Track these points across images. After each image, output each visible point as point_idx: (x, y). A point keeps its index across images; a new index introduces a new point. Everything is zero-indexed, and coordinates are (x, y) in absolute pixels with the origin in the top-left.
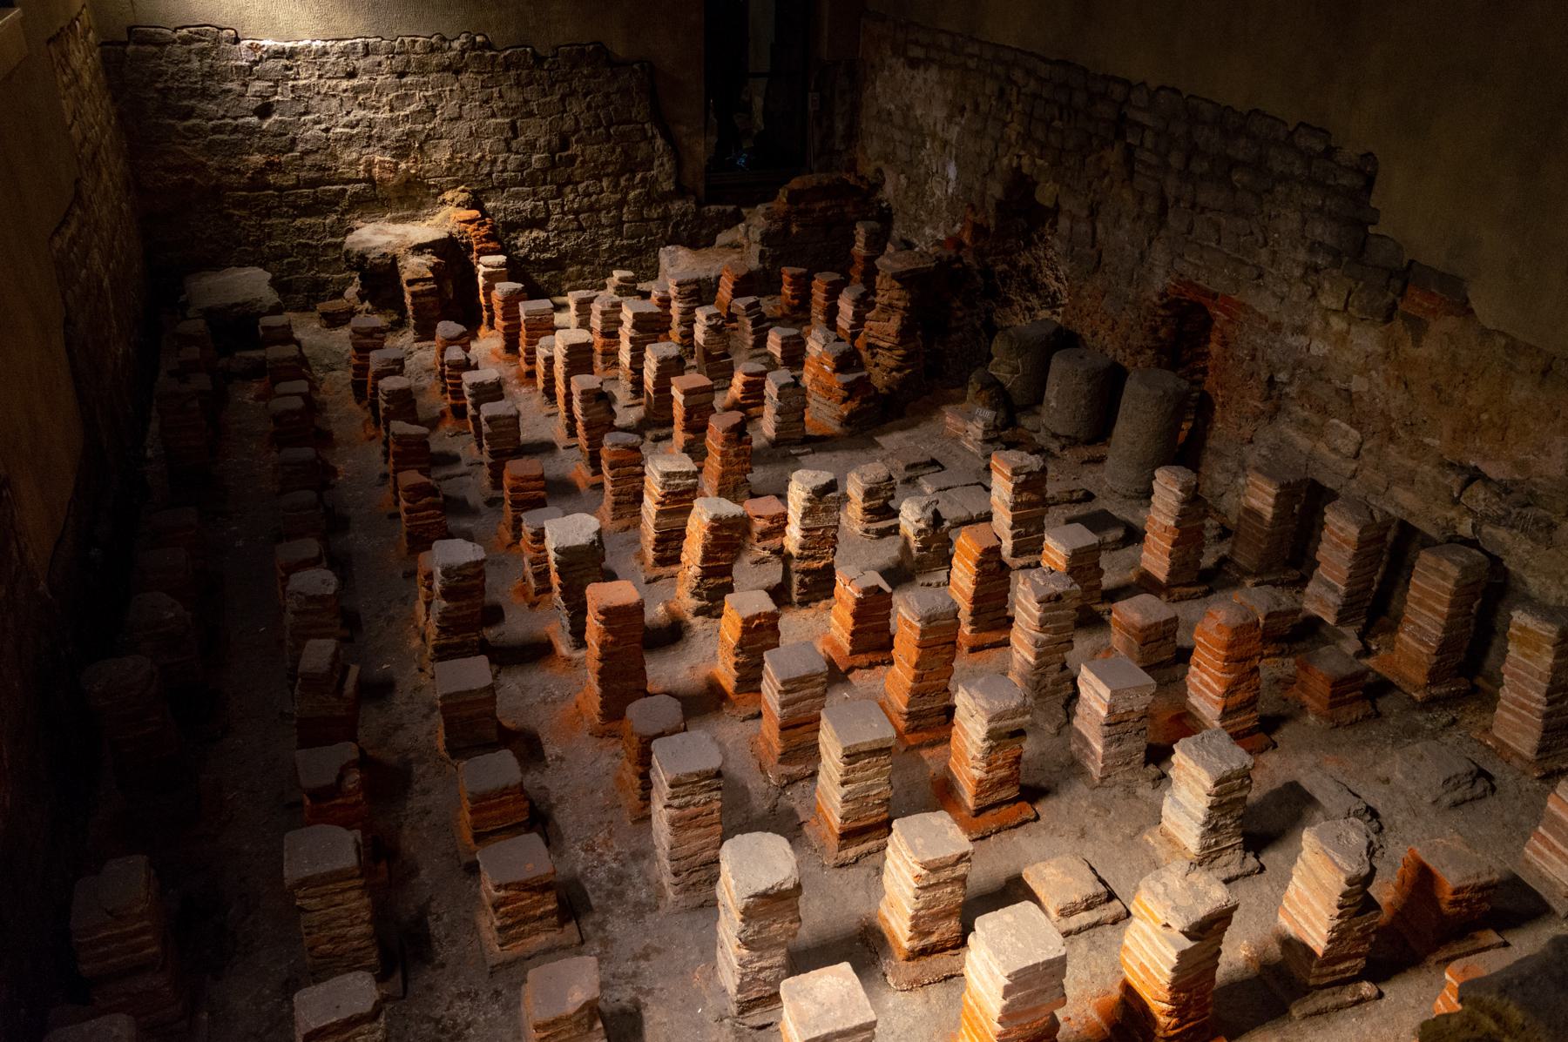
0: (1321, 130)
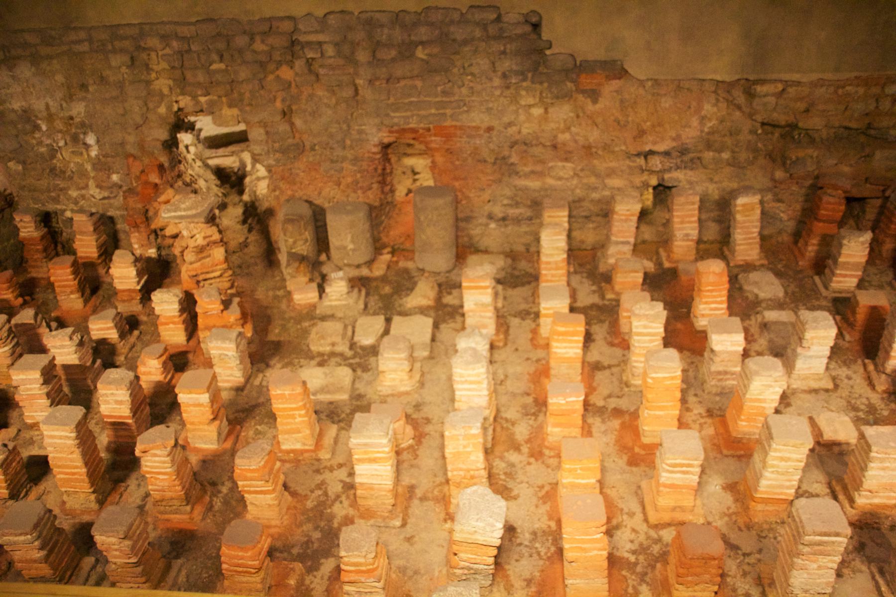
0: (489, 6)
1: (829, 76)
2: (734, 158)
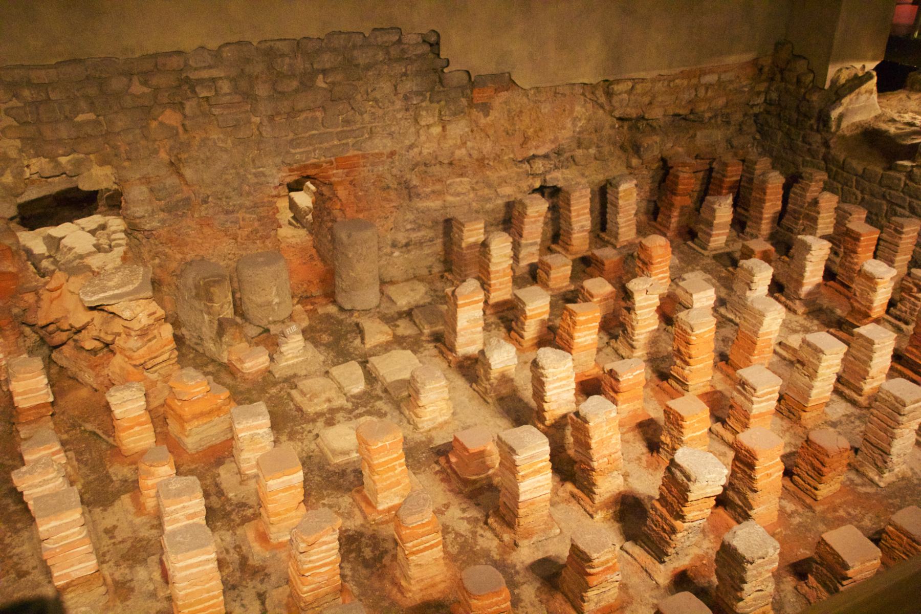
0: (392, 28)
1: (664, 72)
2: (600, 152)
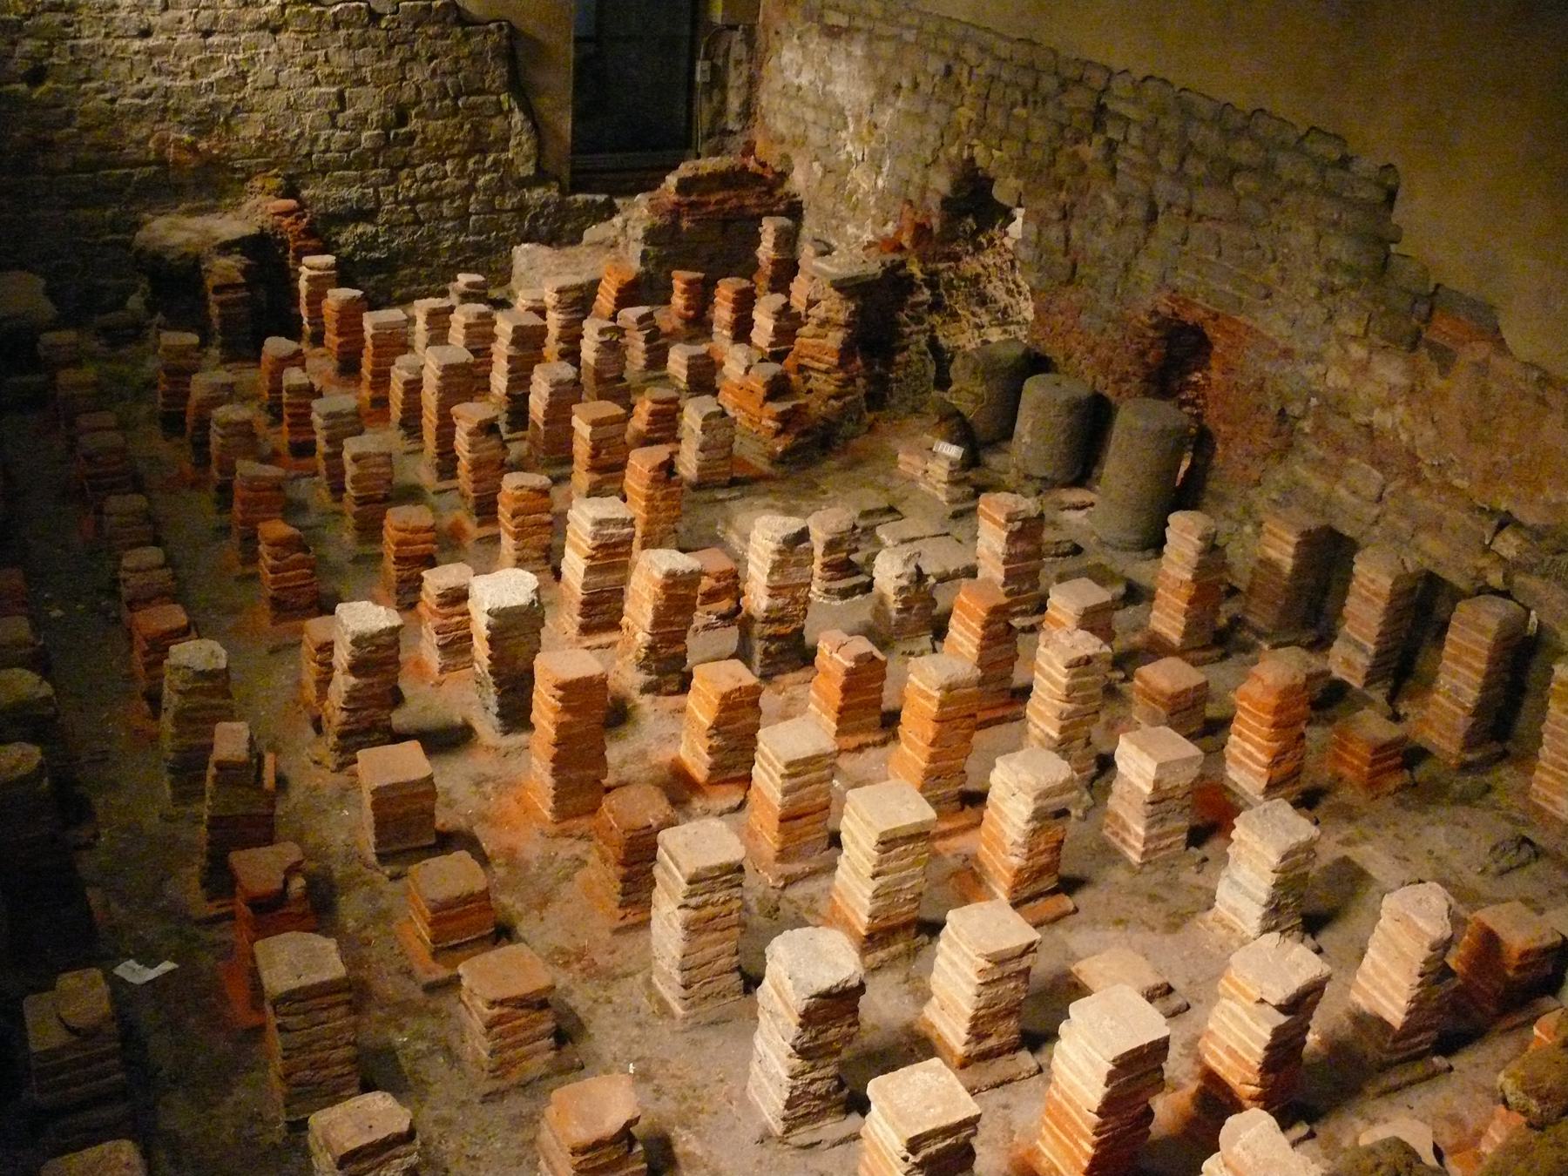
0: (1337, 137)
